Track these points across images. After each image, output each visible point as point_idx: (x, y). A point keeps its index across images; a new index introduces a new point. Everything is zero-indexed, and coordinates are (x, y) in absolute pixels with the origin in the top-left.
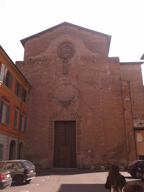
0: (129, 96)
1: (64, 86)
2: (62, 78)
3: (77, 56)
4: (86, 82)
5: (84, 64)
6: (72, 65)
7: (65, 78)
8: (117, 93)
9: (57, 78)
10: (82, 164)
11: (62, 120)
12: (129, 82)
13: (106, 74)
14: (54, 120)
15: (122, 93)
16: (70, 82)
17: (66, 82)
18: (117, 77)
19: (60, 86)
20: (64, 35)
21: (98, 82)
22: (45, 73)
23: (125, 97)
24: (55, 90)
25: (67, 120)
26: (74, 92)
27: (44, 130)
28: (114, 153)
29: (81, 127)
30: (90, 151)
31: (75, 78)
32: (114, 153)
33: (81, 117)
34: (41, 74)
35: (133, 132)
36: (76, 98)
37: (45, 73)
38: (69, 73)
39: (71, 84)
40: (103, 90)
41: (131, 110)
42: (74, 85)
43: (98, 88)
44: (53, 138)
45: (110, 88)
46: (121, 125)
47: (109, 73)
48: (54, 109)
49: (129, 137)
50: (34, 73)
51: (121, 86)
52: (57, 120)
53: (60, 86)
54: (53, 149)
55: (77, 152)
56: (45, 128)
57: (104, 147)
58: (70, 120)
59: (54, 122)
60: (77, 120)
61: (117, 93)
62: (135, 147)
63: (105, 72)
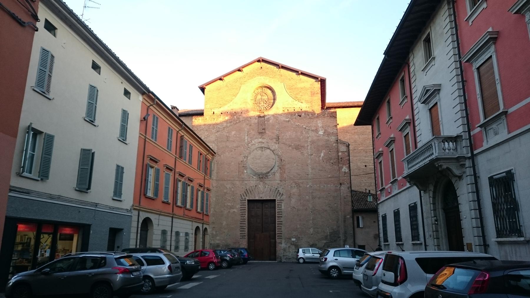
0: (347, 166)
1: (260, 152)
2: (256, 140)
3: (277, 108)
4: (290, 146)
5: (287, 120)
6: (271, 121)
7: (260, 140)
8: (332, 161)
9: (249, 140)
10: (284, 256)
11: (257, 198)
12: (348, 146)
13: (317, 135)
14: (247, 198)
15: (339, 161)
16: (268, 146)
17: (263, 145)
18: (333, 139)
19: (254, 150)
20: (259, 77)
21: (306, 145)
22: (233, 133)
23: (342, 167)
24: (247, 157)
25: (265, 199)
26: (273, 159)
27: (234, 212)
28: (325, 241)
29: (283, 207)
30: (293, 239)
31: (275, 140)
32: (325, 241)
33: (282, 194)
34: (228, 134)
35: (351, 215)
36: (276, 168)
37: (233, 133)
38: (267, 132)
39: (269, 148)
40: (312, 156)
41: (349, 185)
42: (274, 150)
43: (306, 154)
44: (246, 223)
45: (322, 155)
46: (335, 205)
47: (321, 133)
48: (246, 184)
49: (345, 221)
50: (219, 133)
51: (338, 152)
52: (251, 199)
53: (254, 150)
54: (246, 237)
55: (278, 241)
56: (235, 210)
57: (312, 234)
58: (268, 198)
59: (247, 201)
60: (278, 198)
61: (332, 161)
62: (352, 234)
63: (316, 131)
